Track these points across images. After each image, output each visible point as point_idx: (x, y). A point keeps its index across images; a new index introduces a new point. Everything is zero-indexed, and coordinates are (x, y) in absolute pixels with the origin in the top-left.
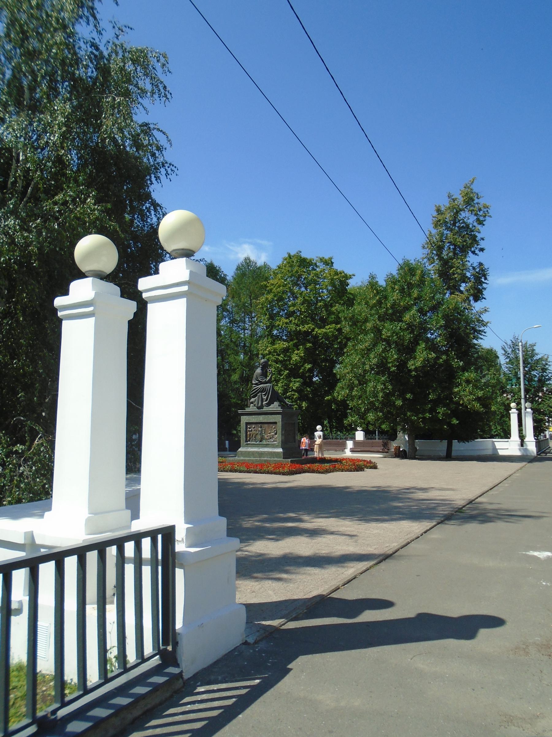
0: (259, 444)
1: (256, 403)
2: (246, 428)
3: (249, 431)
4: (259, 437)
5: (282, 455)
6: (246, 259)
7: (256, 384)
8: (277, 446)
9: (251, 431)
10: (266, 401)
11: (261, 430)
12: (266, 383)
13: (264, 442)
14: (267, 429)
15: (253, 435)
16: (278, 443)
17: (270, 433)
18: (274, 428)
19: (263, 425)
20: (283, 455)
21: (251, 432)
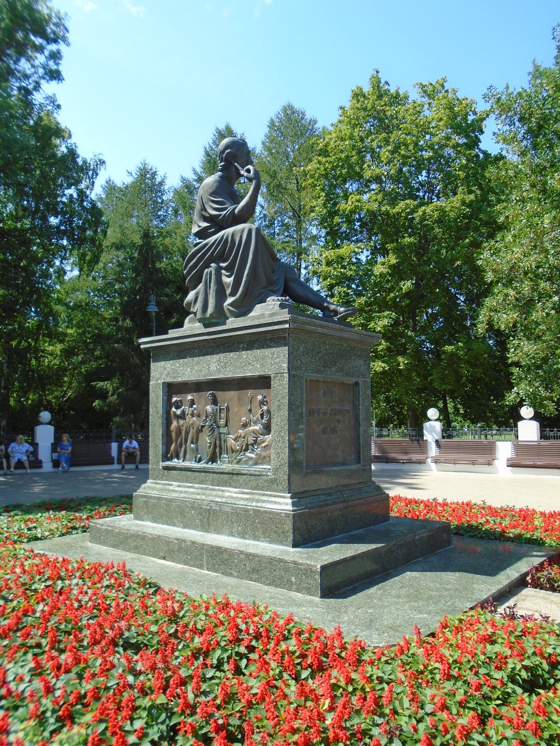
0: (205, 471)
1: (199, 306)
2: (168, 404)
3: (178, 417)
4: (206, 439)
5: (289, 526)
6: (285, 110)
7: (202, 234)
8: (273, 481)
9: (183, 416)
10: (233, 294)
11: (214, 414)
12: (235, 219)
13: (223, 464)
14: (234, 409)
15: (187, 433)
16: (276, 470)
17: (245, 426)
18: (262, 403)
19: (220, 395)
20: (295, 529)
21: (181, 422)
